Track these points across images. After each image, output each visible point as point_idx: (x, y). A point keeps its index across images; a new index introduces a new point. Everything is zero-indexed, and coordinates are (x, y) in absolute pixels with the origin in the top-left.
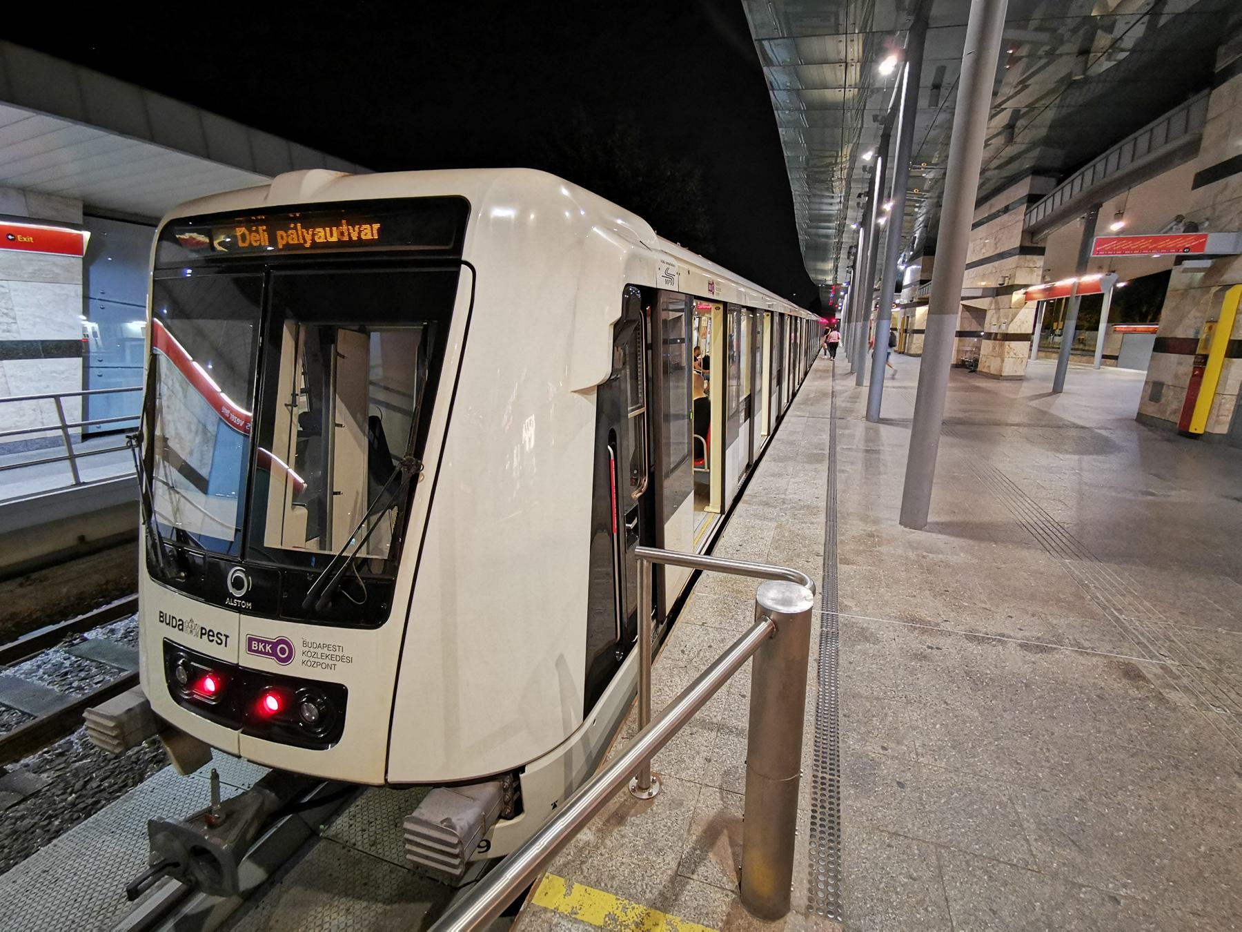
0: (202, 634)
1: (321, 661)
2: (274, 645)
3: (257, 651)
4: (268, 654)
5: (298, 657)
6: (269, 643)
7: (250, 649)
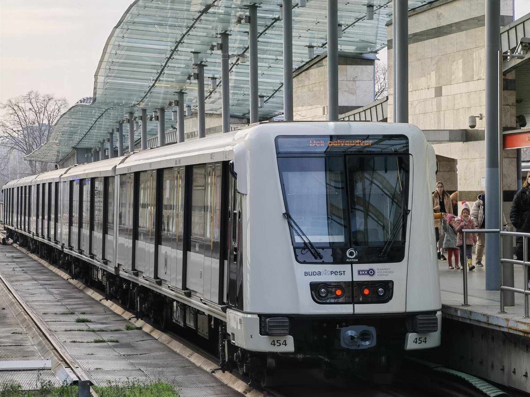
0: (331, 274)
1: (384, 274)
2: (368, 271)
3: (362, 274)
4: (366, 274)
5: (376, 274)
6: (366, 271)
7: (359, 274)
